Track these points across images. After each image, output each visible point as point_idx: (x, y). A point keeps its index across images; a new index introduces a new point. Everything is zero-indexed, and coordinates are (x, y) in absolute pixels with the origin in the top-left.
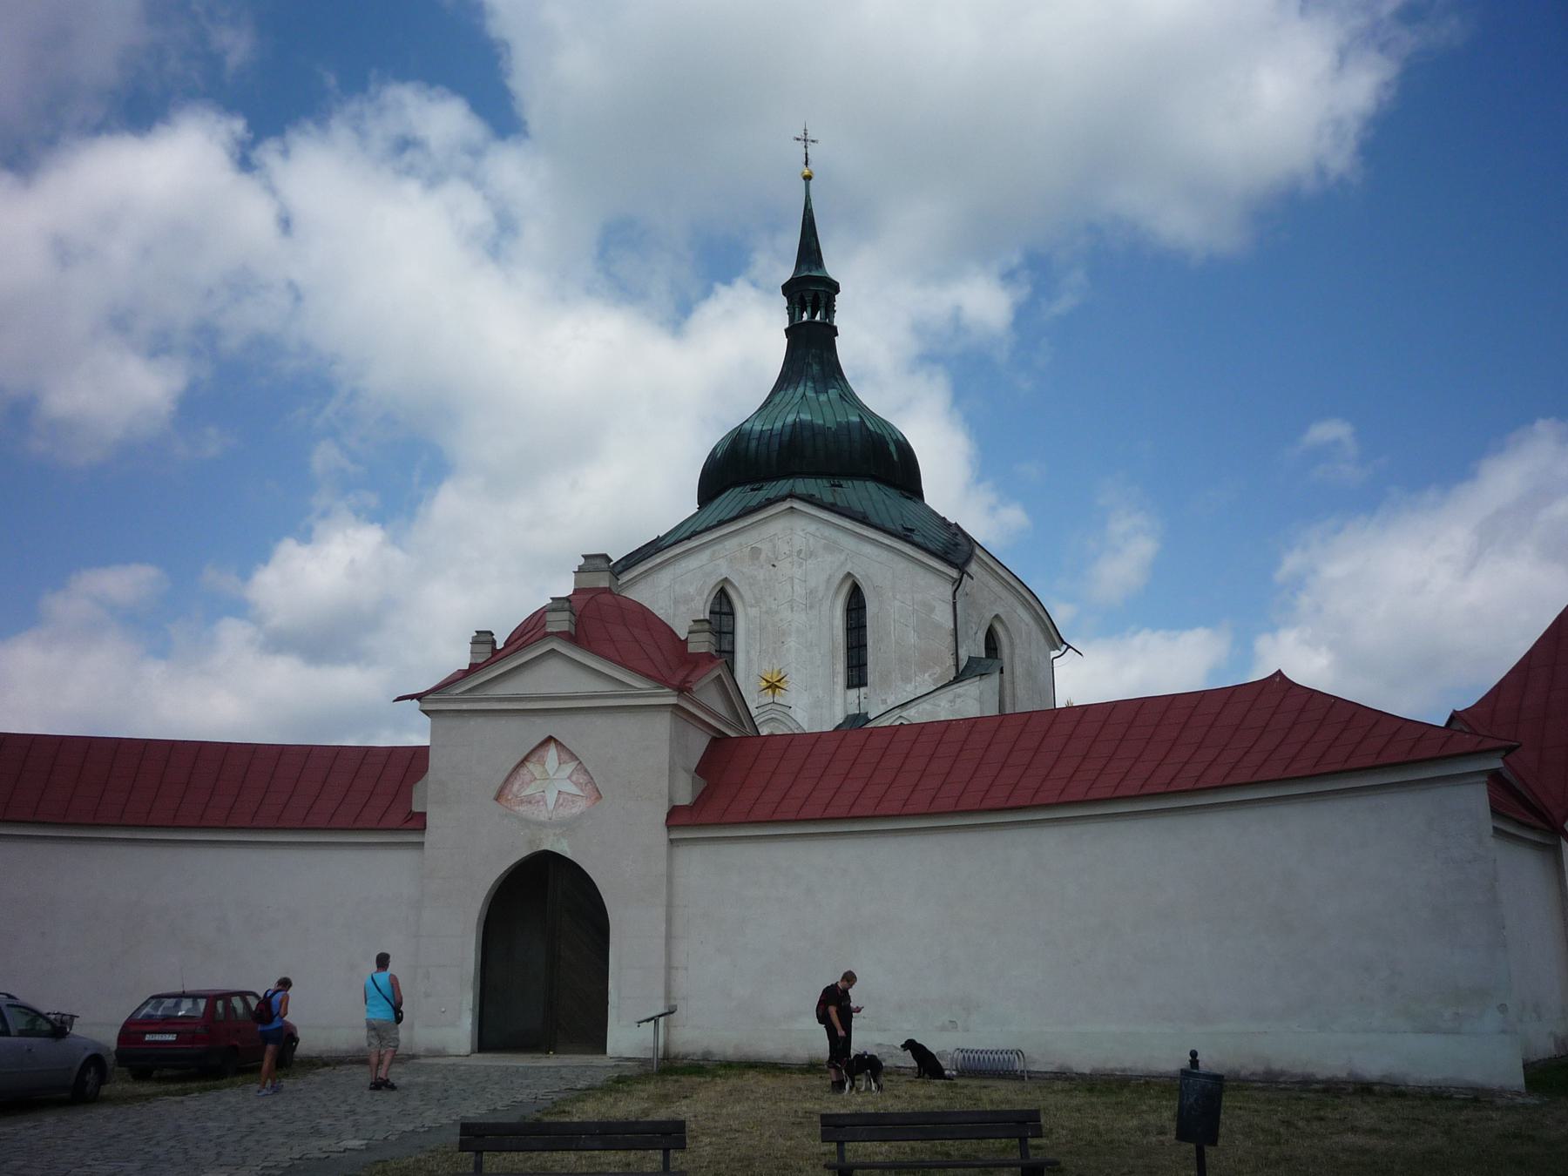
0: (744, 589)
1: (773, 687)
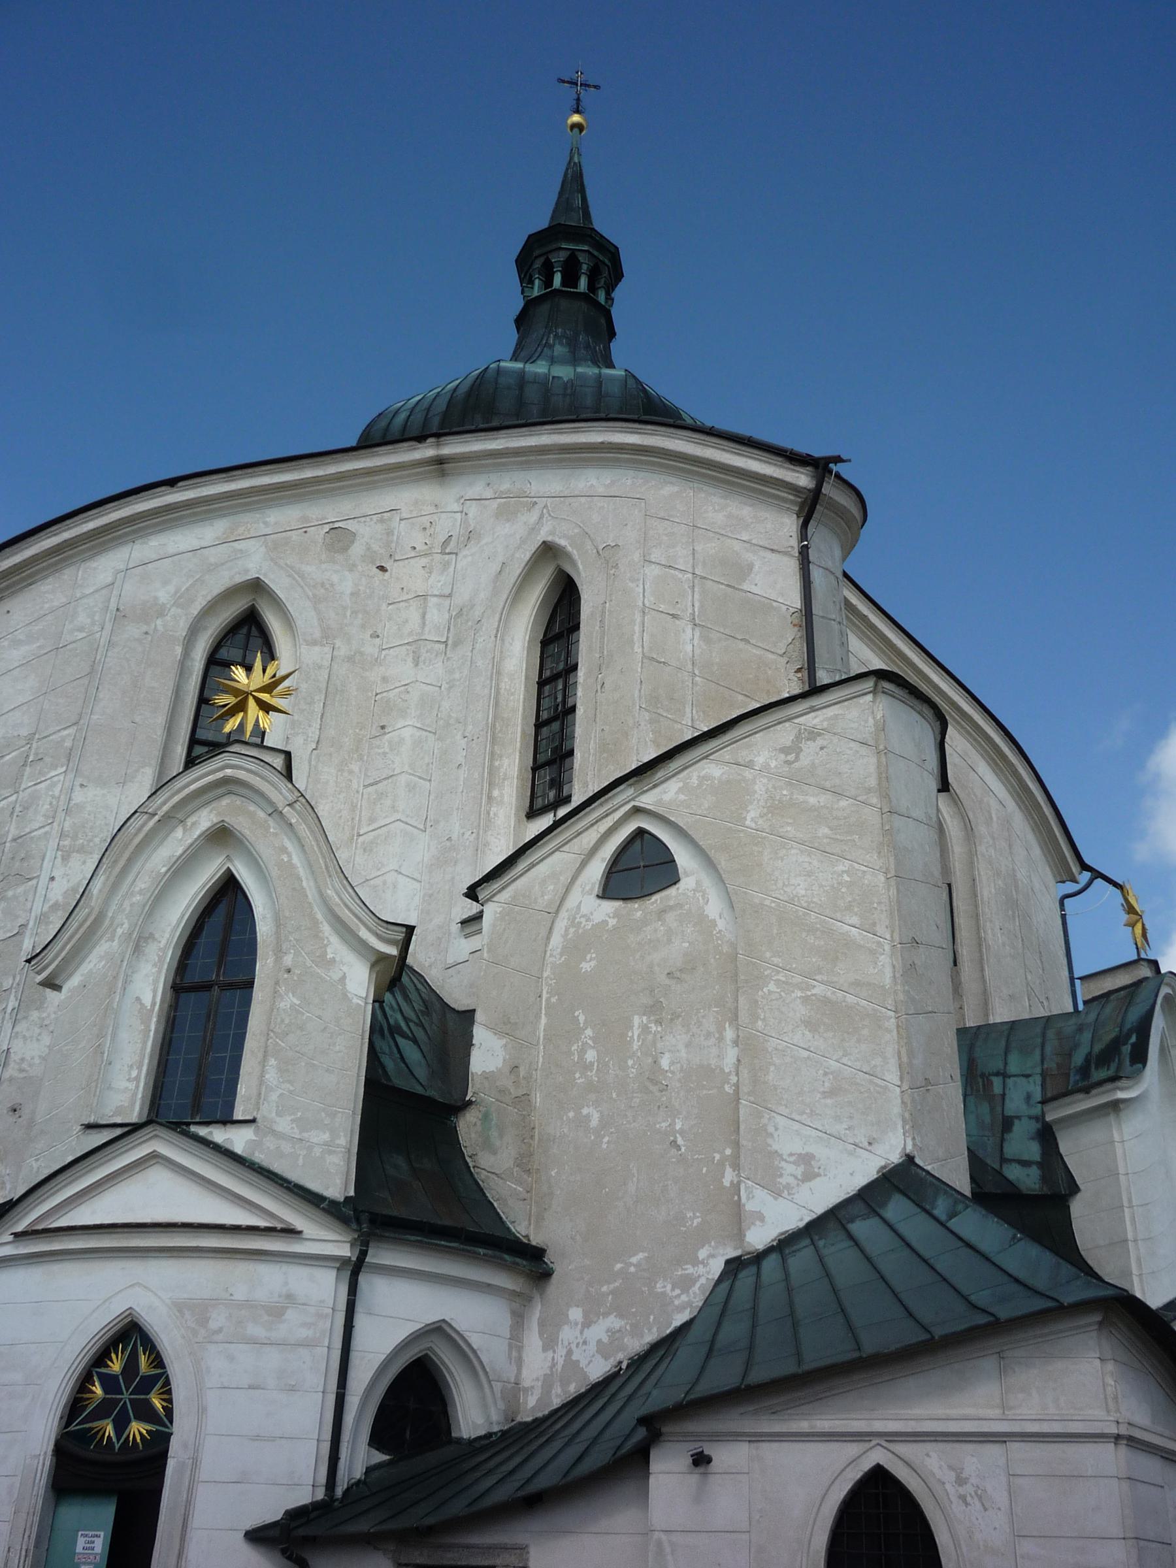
1: (251, 703)
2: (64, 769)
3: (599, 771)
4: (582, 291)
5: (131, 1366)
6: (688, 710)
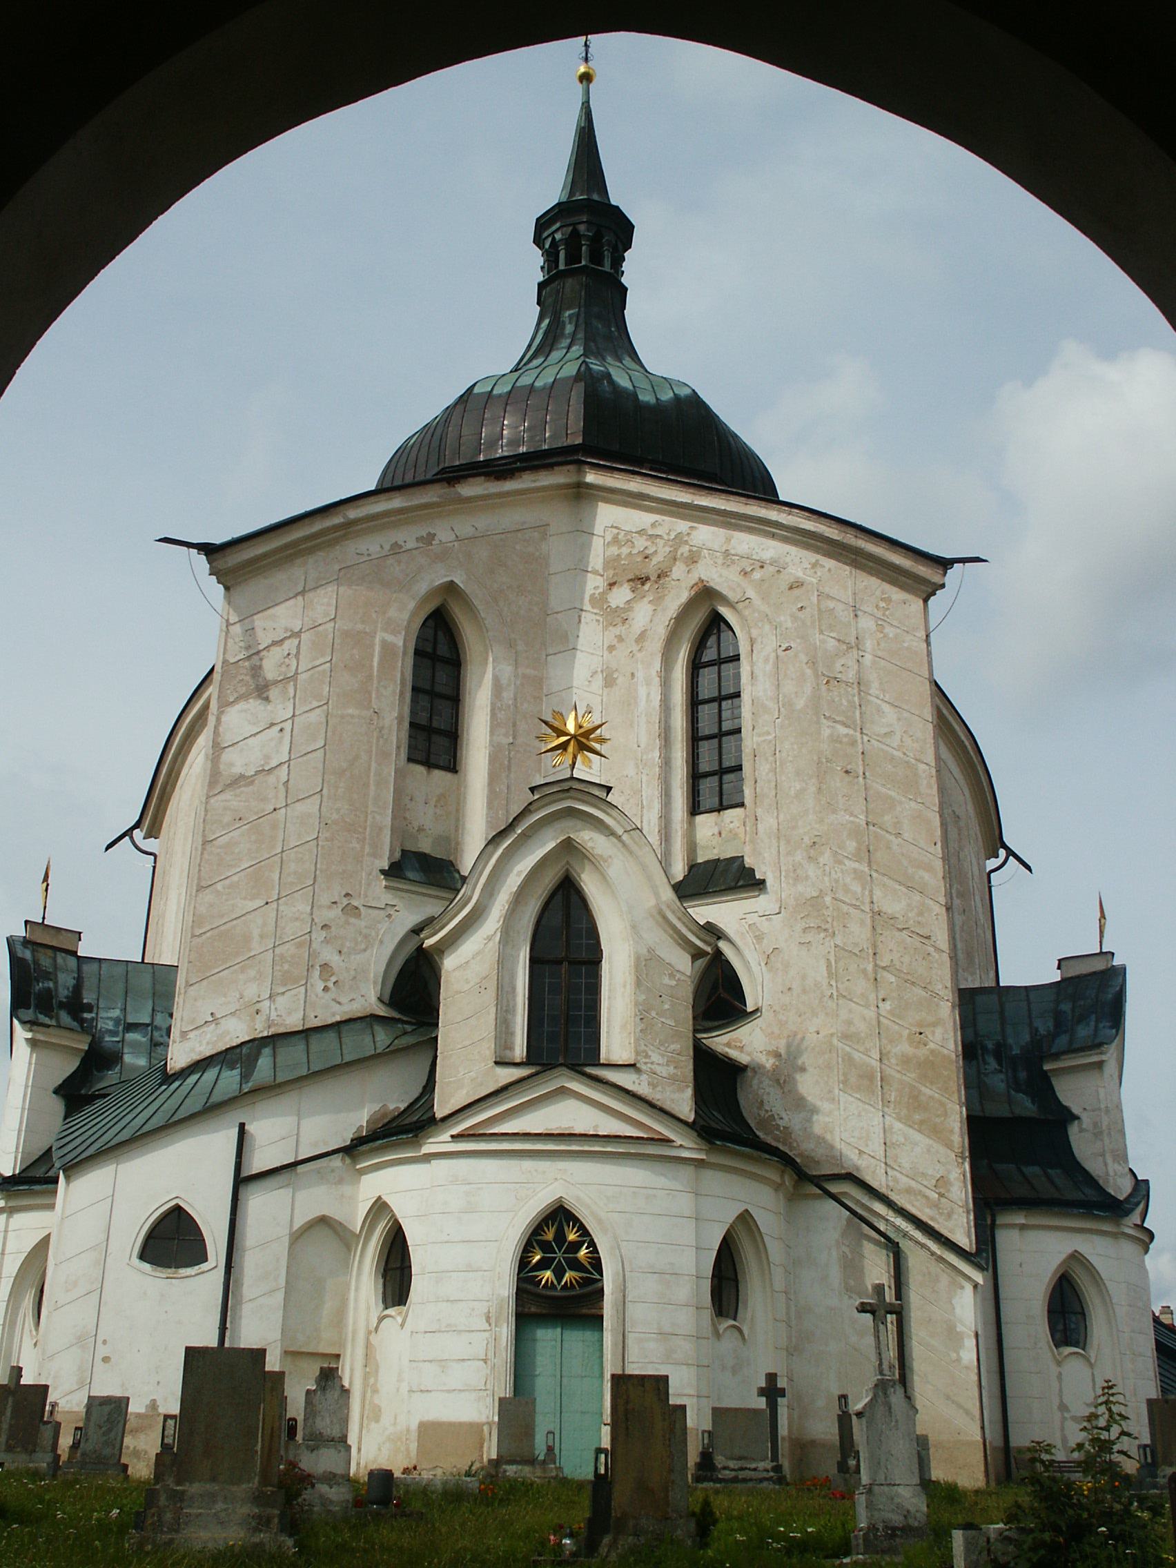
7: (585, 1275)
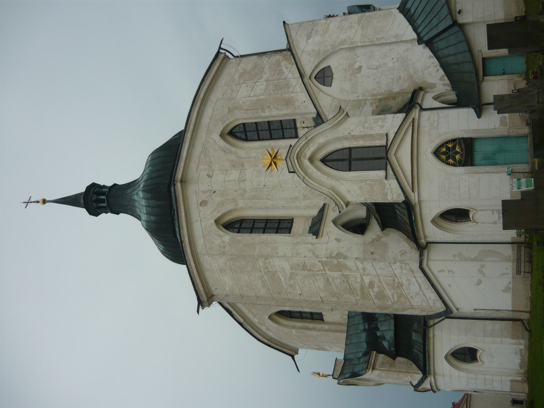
0: (224, 210)
2: (271, 259)
3: (292, 105)
4: (108, 190)
5: (444, 153)
6: (280, 81)
7: (457, 145)
